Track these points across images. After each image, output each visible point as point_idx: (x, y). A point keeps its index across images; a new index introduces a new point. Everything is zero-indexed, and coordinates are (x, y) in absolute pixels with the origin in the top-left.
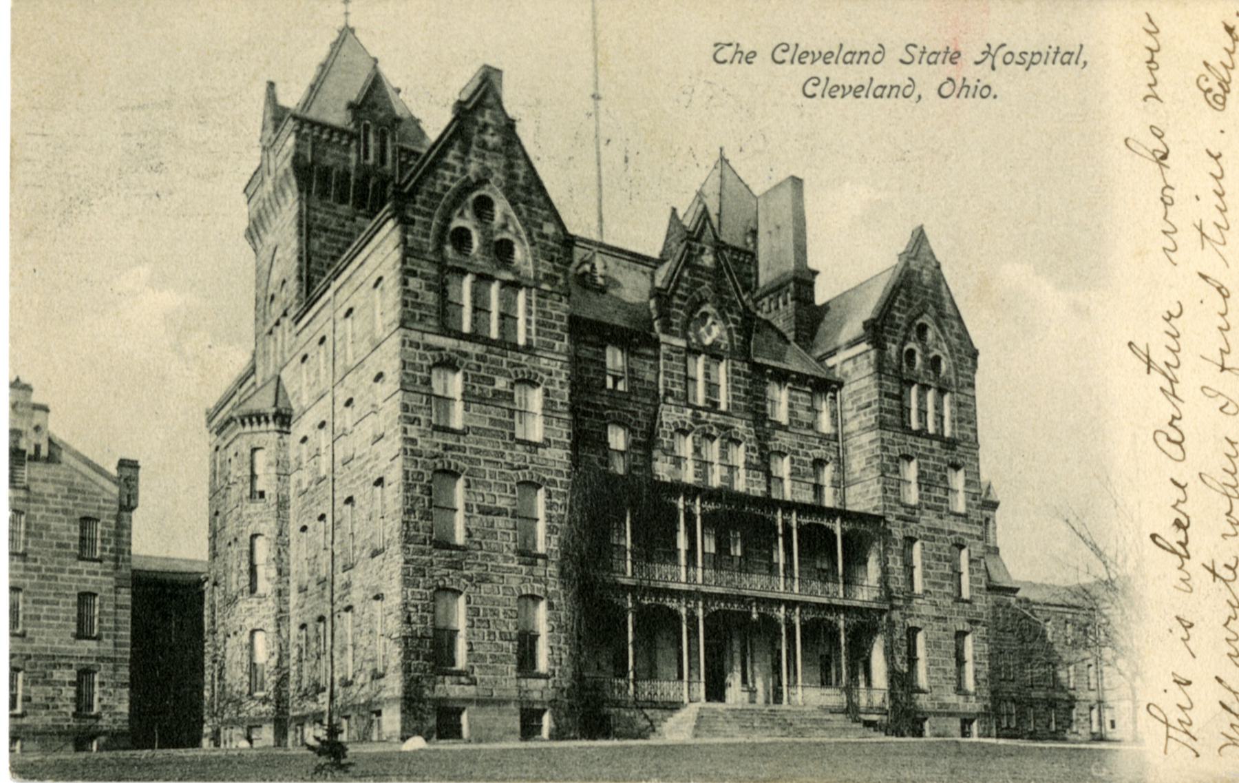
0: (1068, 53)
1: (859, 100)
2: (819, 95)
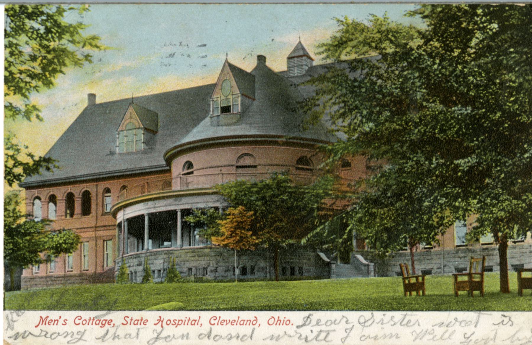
0: (194, 320)
1: (233, 326)
2: (216, 324)
